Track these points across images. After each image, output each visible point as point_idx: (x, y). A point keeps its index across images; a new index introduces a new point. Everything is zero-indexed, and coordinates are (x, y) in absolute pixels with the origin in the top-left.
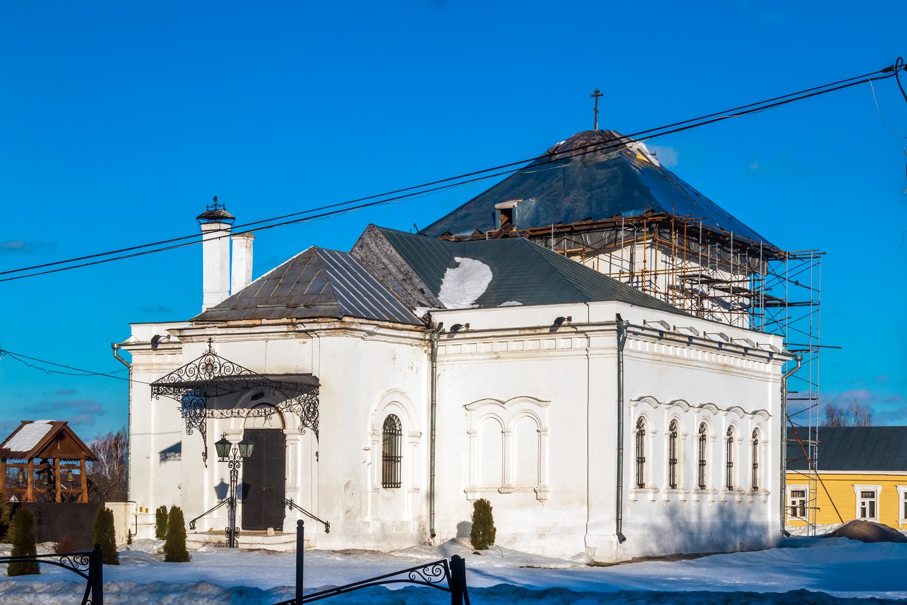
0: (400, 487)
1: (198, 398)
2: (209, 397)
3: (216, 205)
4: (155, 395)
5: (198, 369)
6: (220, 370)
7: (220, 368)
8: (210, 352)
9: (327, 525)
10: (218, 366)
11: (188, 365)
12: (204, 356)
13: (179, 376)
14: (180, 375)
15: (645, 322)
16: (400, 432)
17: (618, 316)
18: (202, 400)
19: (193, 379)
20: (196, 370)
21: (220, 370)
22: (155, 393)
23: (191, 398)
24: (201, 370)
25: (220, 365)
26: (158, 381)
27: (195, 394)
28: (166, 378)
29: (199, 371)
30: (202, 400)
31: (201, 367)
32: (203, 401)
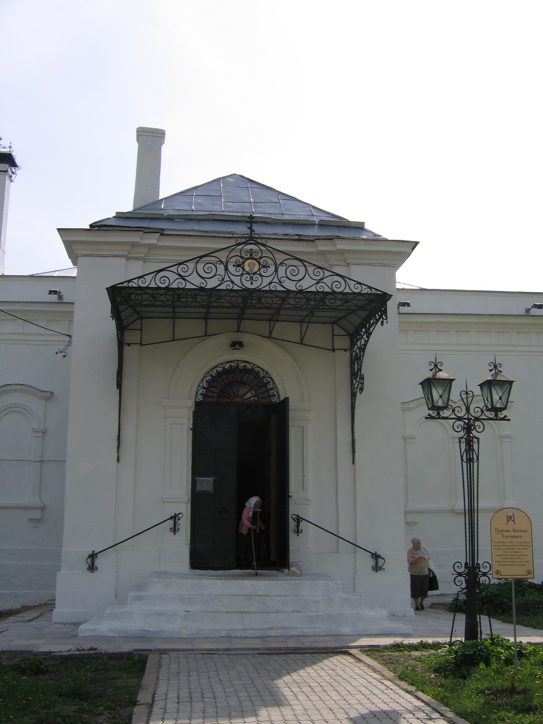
5: (226, 269)
6: (276, 271)
13: (180, 275)
19: (212, 284)
20: (221, 268)
21: (276, 271)
24: (231, 267)
26: (129, 281)
28: (149, 278)
29: (226, 269)
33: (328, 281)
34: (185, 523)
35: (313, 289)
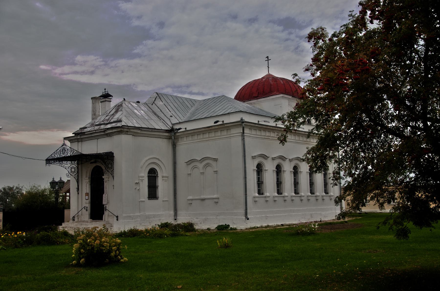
0: (158, 199)
1: (73, 165)
2: (79, 164)
3: (105, 92)
4: (48, 164)
5: (60, 152)
7: (67, 150)
8: (64, 144)
9: (117, 217)
10: (67, 150)
11: (57, 150)
12: (62, 146)
14: (55, 155)
15: (259, 121)
16: (157, 175)
17: (242, 119)
18: (76, 166)
19: (59, 156)
20: (60, 152)
22: (48, 163)
23: (69, 165)
24: (61, 152)
25: (67, 149)
27: (71, 163)
28: (50, 156)
29: (60, 153)
30: (76, 166)
31: (61, 151)
32: (76, 166)
33: (74, 152)
34: (89, 209)
35: (72, 155)
